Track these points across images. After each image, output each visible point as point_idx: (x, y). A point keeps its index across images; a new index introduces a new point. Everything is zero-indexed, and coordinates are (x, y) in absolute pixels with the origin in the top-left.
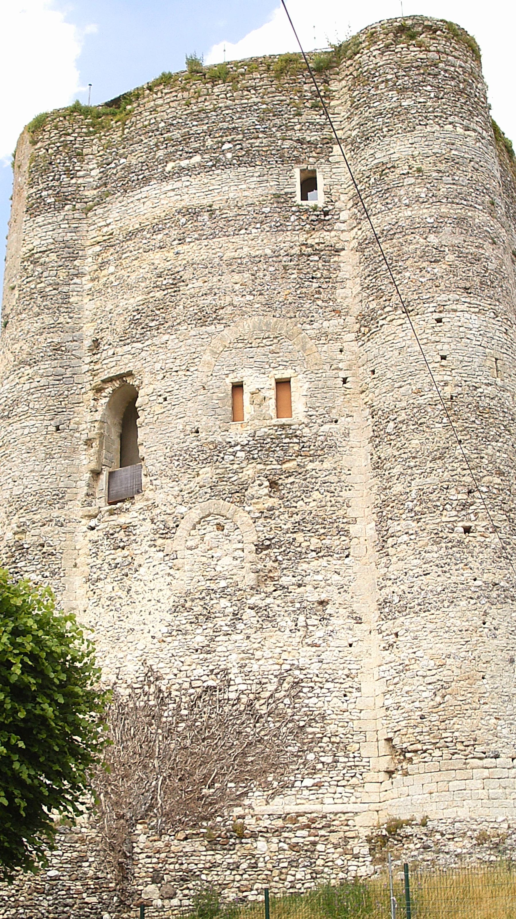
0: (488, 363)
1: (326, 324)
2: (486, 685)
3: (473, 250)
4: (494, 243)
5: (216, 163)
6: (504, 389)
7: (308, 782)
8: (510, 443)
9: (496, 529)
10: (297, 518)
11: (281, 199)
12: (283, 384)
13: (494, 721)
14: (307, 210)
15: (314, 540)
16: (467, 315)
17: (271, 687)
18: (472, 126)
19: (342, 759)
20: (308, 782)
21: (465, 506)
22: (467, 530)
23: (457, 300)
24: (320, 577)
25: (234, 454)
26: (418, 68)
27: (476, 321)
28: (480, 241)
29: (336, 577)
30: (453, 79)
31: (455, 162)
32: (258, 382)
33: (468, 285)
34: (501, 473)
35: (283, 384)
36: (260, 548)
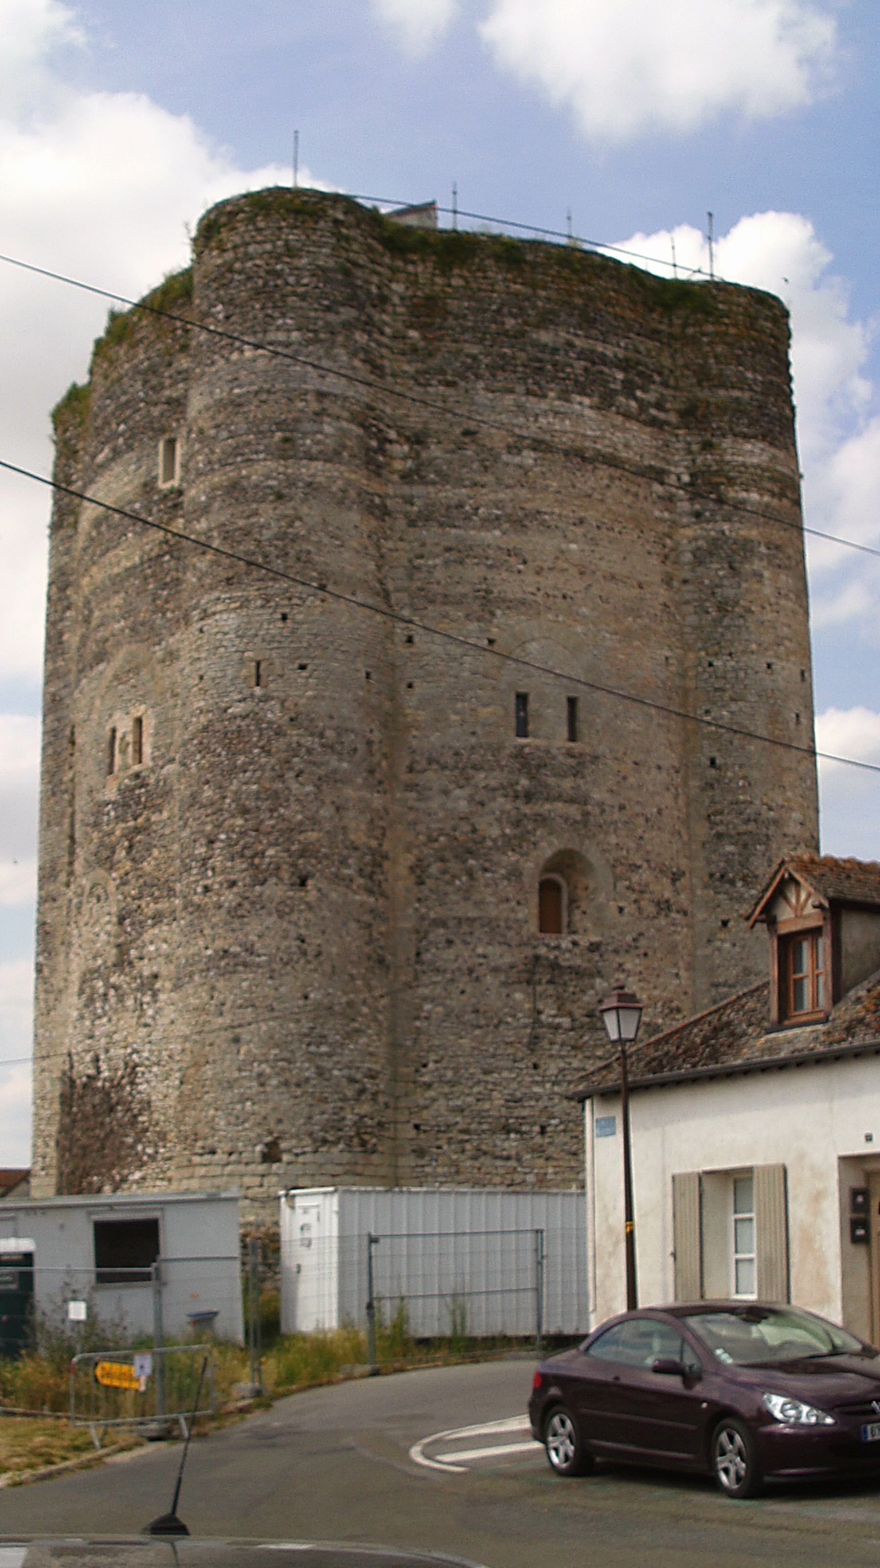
0: (244, 672)
1: (171, 640)
2: (208, 1071)
3: (241, 523)
4: (280, 497)
5: (116, 453)
6: (266, 699)
7: (137, 1175)
8: (269, 767)
9: (233, 884)
10: (141, 881)
11: (148, 486)
12: (139, 722)
13: (212, 1112)
14: (166, 496)
15: (152, 905)
16: (225, 616)
17: (120, 1073)
18: (271, 336)
19: (162, 1150)
20: (137, 1175)
21: (204, 861)
22: (207, 889)
23: (218, 599)
24: (152, 948)
25: (108, 814)
26: (214, 280)
27: (229, 621)
28: (254, 506)
29: (165, 946)
30: (249, 278)
31: (236, 404)
32: (124, 726)
33: (231, 574)
34: (244, 811)
35: (139, 722)
36: (121, 920)
